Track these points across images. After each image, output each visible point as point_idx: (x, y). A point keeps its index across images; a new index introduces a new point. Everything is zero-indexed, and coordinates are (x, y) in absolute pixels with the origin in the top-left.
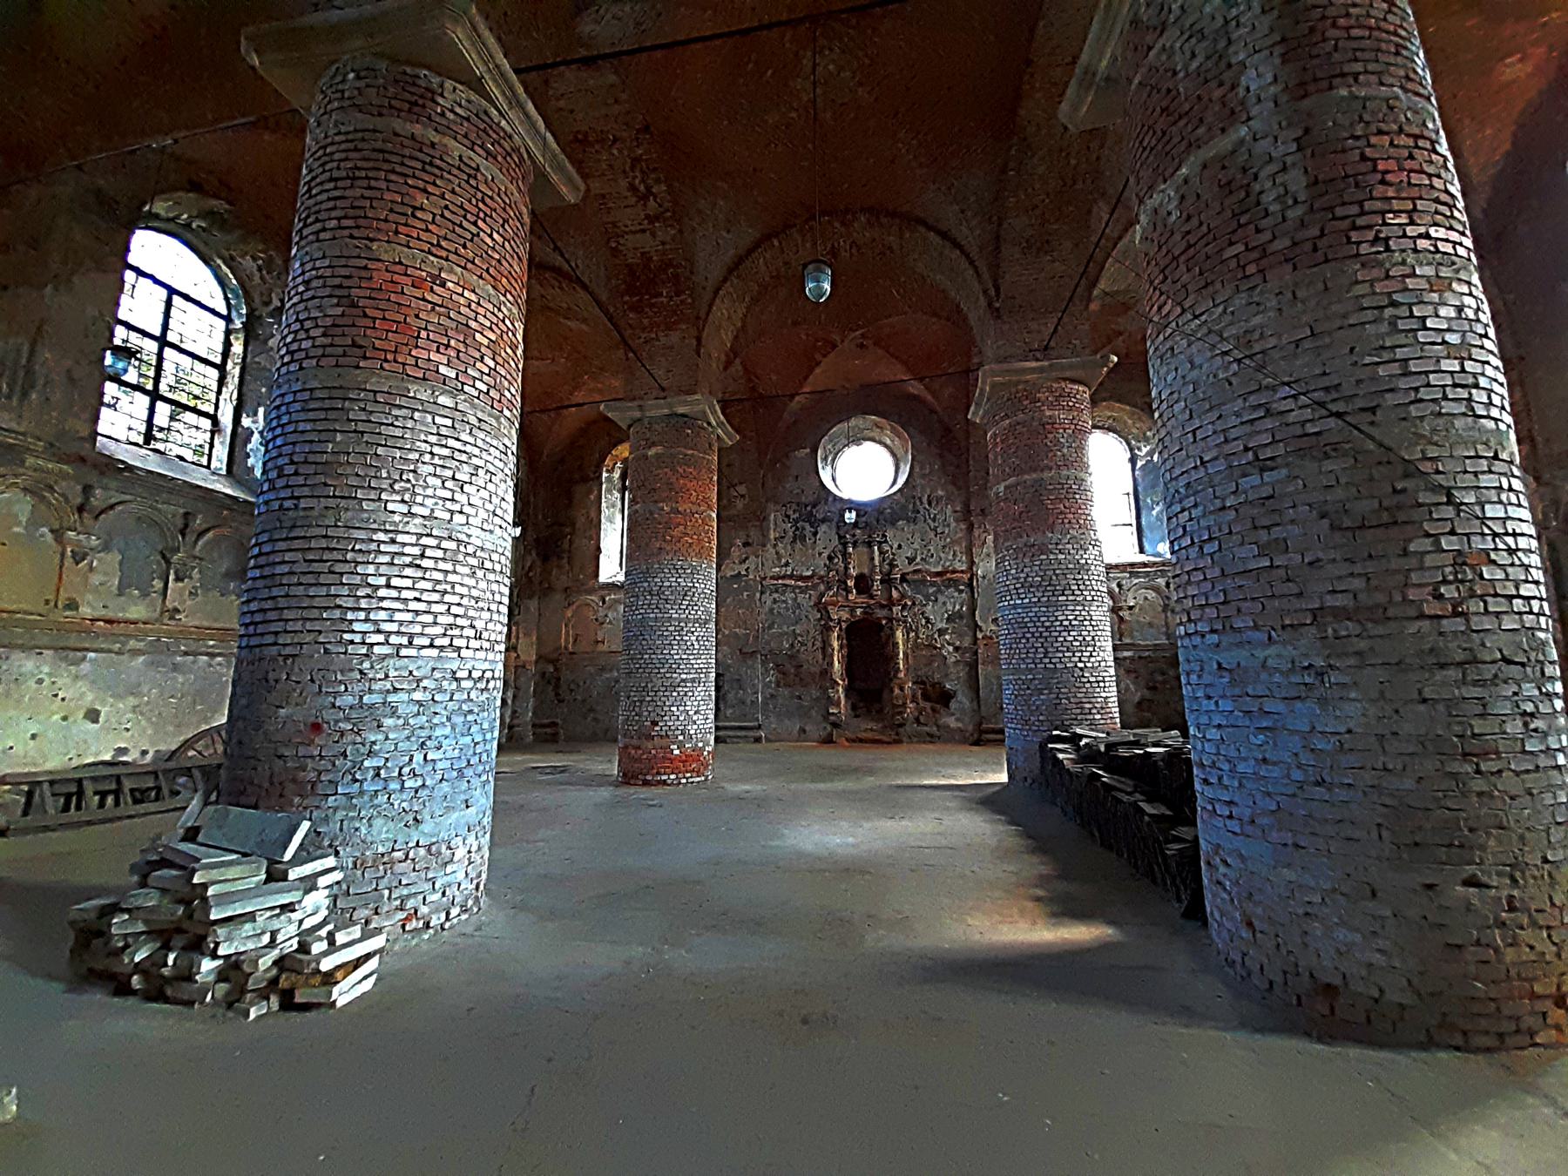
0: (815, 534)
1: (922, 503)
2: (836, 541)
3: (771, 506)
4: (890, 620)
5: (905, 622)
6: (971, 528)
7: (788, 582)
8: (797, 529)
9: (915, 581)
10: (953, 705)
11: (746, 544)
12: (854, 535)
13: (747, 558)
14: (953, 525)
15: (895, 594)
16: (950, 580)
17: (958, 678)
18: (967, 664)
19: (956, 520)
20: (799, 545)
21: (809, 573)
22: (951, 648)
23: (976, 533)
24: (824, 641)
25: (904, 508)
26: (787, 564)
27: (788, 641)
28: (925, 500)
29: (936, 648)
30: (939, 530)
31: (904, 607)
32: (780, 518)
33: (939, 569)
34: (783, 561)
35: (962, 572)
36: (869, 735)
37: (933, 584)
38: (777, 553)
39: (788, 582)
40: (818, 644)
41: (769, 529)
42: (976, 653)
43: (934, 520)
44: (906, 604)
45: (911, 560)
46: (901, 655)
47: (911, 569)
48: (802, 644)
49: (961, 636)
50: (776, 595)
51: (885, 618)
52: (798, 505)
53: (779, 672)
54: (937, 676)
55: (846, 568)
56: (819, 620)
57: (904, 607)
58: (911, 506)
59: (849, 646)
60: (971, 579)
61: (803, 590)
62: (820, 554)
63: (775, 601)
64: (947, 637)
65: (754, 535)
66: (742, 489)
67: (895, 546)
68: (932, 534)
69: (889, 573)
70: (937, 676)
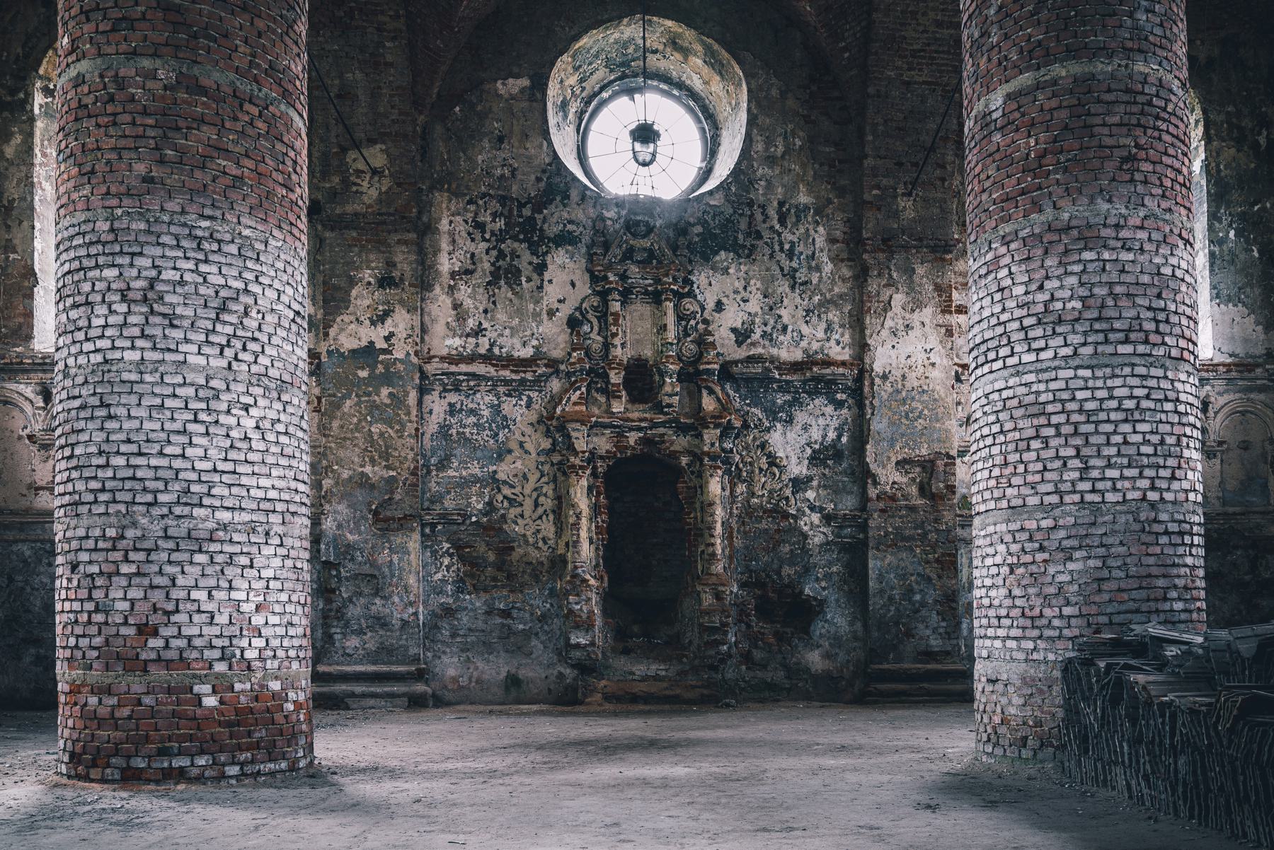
0: (541, 268)
1: (766, 218)
2: (584, 289)
3: (440, 198)
4: (697, 457)
5: (727, 462)
6: (861, 276)
7: (480, 368)
8: (501, 255)
9: (749, 380)
10: (819, 628)
11: (385, 282)
12: (623, 277)
13: (387, 314)
14: (828, 267)
15: (708, 404)
16: (817, 379)
17: (828, 576)
18: (844, 548)
19: (835, 259)
20: (504, 292)
21: (527, 352)
22: (816, 518)
23: (873, 286)
24: (559, 498)
25: (728, 224)
26: (478, 332)
27: (480, 495)
28: (772, 213)
29: (786, 516)
30: (801, 276)
31: (727, 430)
32: (462, 228)
33: (798, 355)
34: (471, 323)
35: (843, 364)
36: (654, 688)
37: (785, 387)
38: (456, 306)
39: (480, 368)
40: (548, 503)
41: (437, 251)
42: (864, 527)
43: (791, 255)
44: (729, 426)
45: (742, 335)
46: (719, 529)
47: (741, 353)
48: (512, 502)
49: (836, 491)
50: (453, 398)
52: (503, 200)
53: (461, 558)
54: (787, 571)
55: (607, 346)
56: (548, 452)
57: (727, 430)
58: (743, 225)
59: (611, 511)
60: (859, 379)
61: (515, 389)
62: (551, 313)
63: (452, 409)
64: (811, 495)
65: (404, 261)
66: (377, 156)
67: (710, 305)
68: (783, 287)
69: (699, 357)
70: (787, 571)
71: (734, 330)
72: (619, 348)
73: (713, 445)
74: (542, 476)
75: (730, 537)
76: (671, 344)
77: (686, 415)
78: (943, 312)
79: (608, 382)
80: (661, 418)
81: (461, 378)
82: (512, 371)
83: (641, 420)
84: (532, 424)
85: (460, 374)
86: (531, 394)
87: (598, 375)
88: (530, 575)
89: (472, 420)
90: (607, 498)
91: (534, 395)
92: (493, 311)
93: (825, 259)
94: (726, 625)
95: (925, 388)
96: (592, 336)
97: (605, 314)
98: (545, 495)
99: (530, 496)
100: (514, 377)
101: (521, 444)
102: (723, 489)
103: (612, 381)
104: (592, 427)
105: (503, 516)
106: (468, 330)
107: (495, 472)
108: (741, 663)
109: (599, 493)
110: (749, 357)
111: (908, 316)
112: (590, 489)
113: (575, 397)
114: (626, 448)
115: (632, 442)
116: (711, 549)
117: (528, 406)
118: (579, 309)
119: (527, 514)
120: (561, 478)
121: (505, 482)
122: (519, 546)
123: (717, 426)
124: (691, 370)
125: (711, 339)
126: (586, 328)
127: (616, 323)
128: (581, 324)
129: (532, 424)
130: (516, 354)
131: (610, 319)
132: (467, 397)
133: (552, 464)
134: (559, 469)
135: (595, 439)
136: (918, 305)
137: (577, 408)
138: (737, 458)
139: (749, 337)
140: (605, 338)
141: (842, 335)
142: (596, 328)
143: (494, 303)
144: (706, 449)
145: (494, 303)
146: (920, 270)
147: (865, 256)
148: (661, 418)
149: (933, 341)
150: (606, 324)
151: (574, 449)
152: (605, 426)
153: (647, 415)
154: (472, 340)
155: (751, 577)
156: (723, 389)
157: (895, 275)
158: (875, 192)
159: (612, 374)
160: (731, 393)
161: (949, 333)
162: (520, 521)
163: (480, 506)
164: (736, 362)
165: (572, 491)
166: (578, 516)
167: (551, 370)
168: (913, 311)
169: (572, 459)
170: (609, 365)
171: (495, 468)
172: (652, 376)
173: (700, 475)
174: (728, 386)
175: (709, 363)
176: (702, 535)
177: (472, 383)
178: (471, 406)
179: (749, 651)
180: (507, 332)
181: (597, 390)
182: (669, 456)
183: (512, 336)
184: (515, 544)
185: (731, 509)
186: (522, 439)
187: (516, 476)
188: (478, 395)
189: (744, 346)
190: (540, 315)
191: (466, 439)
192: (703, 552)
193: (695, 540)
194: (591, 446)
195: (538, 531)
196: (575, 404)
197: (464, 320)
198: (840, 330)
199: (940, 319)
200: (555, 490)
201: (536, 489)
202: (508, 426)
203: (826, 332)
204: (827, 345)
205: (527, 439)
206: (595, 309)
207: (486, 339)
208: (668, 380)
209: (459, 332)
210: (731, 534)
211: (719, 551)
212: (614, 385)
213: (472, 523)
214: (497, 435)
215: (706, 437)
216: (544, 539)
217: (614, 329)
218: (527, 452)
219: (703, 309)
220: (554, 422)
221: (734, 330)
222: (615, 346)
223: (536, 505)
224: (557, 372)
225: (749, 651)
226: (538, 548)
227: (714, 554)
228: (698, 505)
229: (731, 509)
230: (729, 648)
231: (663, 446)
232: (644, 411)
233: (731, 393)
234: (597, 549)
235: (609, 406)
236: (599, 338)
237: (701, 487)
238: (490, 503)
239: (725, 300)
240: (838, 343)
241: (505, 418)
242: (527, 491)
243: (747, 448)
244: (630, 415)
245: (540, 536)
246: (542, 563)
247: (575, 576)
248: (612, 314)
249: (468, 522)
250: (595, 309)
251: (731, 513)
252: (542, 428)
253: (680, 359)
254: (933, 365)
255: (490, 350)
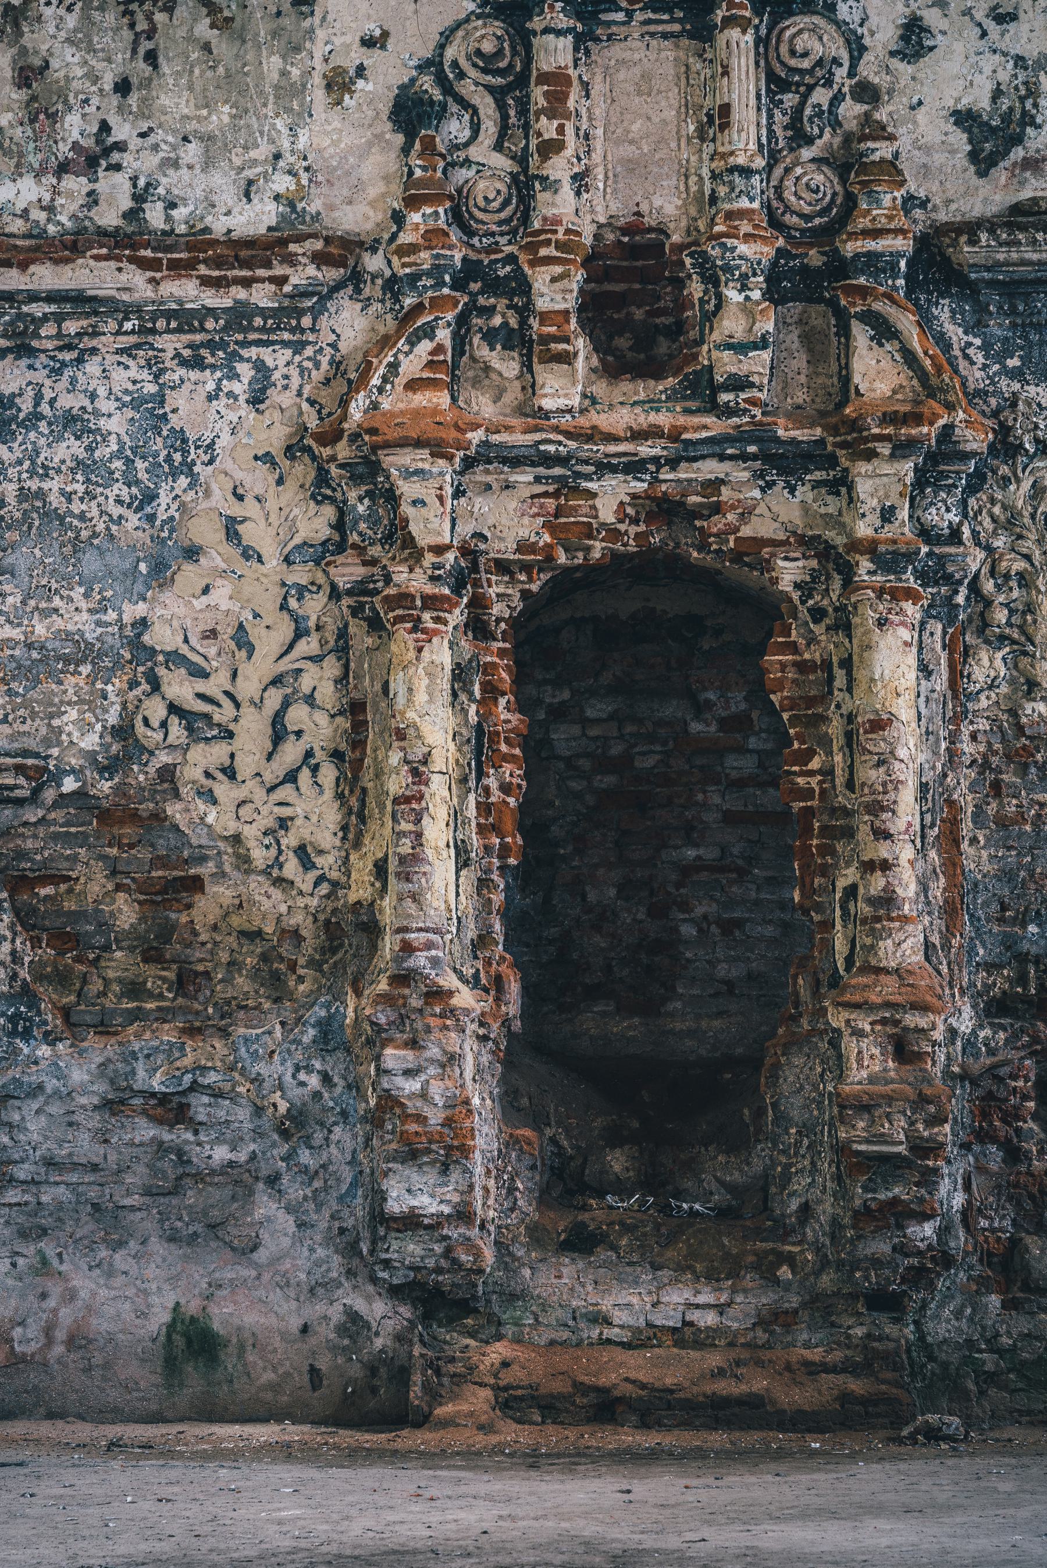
27: (94, 701)
46: (907, 800)
51: (808, 543)
71: (964, 118)
72: (567, 190)
73: (887, 514)
74: (300, 633)
75: (951, 839)
76: (746, 172)
77: (797, 415)
79: (525, 311)
80: (714, 426)
81: (38, 309)
82: (206, 282)
83: (638, 435)
84: (267, 458)
85: (33, 297)
86: (266, 354)
87: (494, 286)
88: (255, 974)
89: (69, 448)
90: (522, 706)
91: (277, 358)
92: (146, 83)
94: (934, 1148)
96: (474, 153)
97: (522, 80)
98: (310, 700)
99: (258, 705)
100: (211, 299)
101: (231, 529)
102: (925, 670)
103: (542, 304)
104: (469, 464)
105: (167, 774)
106: (64, 149)
107: (143, 624)
108: (984, 1285)
109: (491, 691)
110: (1016, 209)
112: (460, 675)
113: (412, 364)
114: (589, 531)
115: (607, 514)
116: (878, 883)
117: (256, 400)
118: (432, 65)
119: (246, 766)
120: (361, 639)
121: (174, 658)
122: (221, 875)
123: (902, 449)
124: (815, 258)
125: (883, 150)
126: (456, 128)
127: (556, 106)
128: (442, 114)
129: (267, 458)
130: (219, 225)
131: (538, 95)
132: (56, 372)
133: (335, 594)
134: (356, 611)
135: (481, 504)
137: (421, 399)
138: (975, 560)
139: (1018, 140)
140: (522, 159)
142: (490, 128)
143: (151, 57)
144: (863, 530)
145: (151, 57)
148: (714, 426)
150: (523, 110)
151: (409, 541)
152: (515, 461)
153: (663, 419)
154: (76, 184)
155: (1022, 979)
156: (925, 322)
159: (540, 279)
160: (955, 333)
162: (222, 789)
163: (90, 741)
164: (970, 229)
165: (398, 685)
166: (418, 772)
167: (333, 274)
169: (401, 574)
170: (532, 248)
171: (141, 609)
172: (679, 283)
173: (844, 625)
174: (943, 312)
175: (876, 233)
176: (849, 833)
177: (71, 327)
178: (68, 402)
179: (1014, 1243)
180: (192, 152)
181: (490, 336)
182: (737, 556)
183: (208, 164)
184: (207, 869)
185: (953, 738)
186: (236, 510)
187: (212, 634)
188: (92, 367)
189: (1000, 174)
190: (300, 90)
191: (50, 515)
192: (851, 891)
193: (827, 850)
194: (465, 529)
195: (284, 823)
196: (413, 385)
197: (53, 117)
200: (341, 681)
201: (276, 681)
202: (188, 468)
205: (250, 508)
206: (487, 63)
207: (121, 179)
208: (733, 295)
209: (35, 160)
210: (952, 824)
211: (907, 886)
212: (545, 317)
213: (63, 800)
214: (150, 497)
215: (863, 488)
216: (302, 851)
217: (548, 128)
218: (250, 554)
219: (857, 48)
220: (343, 450)
221: (964, 118)
222: (551, 186)
223: (279, 733)
224: (356, 278)
225: (1014, 1243)
226: (280, 882)
227: (888, 900)
228: (835, 728)
229: (953, 738)
230: (945, 1231)
231: (717, 524)
232: (652, 404)
233: (955, 333)
234: (483, 884)
235: (531, 388)
236: (502, 162)
237: (847, 664)
238: (123, 731)
239: (932, 17)
241: (180, 440)
242: (248, 687)
243: (1010, 523)
244: (603, 420)
245: (290, 840)
246: (296, 935)
247: (403, 979)
248: (544, 78)
249: (49, 795)
250: (487, 63)
251: (952, 754)
252: (302, 471)
253: (775, 223)
255: (133, 215)
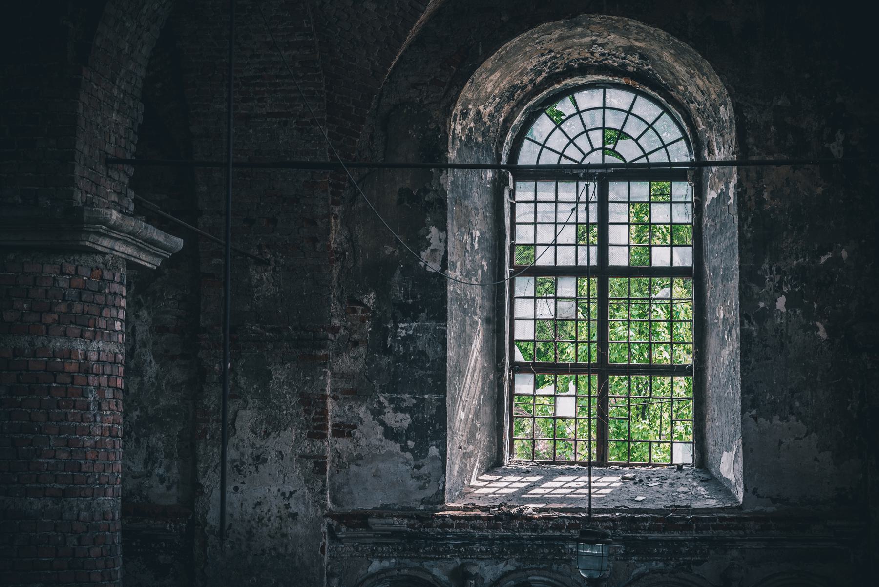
14: (152, 369)
78: (312, 436)
93: (149, 358)
95: (282, 550)
111: (259, 442)
136: (275, 425)
141: (168, 469)
146: (279, 374)
147: (201, 354)
149: (295, 480)
157: (242, 381)
158: (215, 261)
161: (320, 467)
168: (267, 434)
198: (166, 461)
199: (307, 447)
203: (146, 464)
204: (147, 483)
240: (162, 480)
254: (294, 516)
